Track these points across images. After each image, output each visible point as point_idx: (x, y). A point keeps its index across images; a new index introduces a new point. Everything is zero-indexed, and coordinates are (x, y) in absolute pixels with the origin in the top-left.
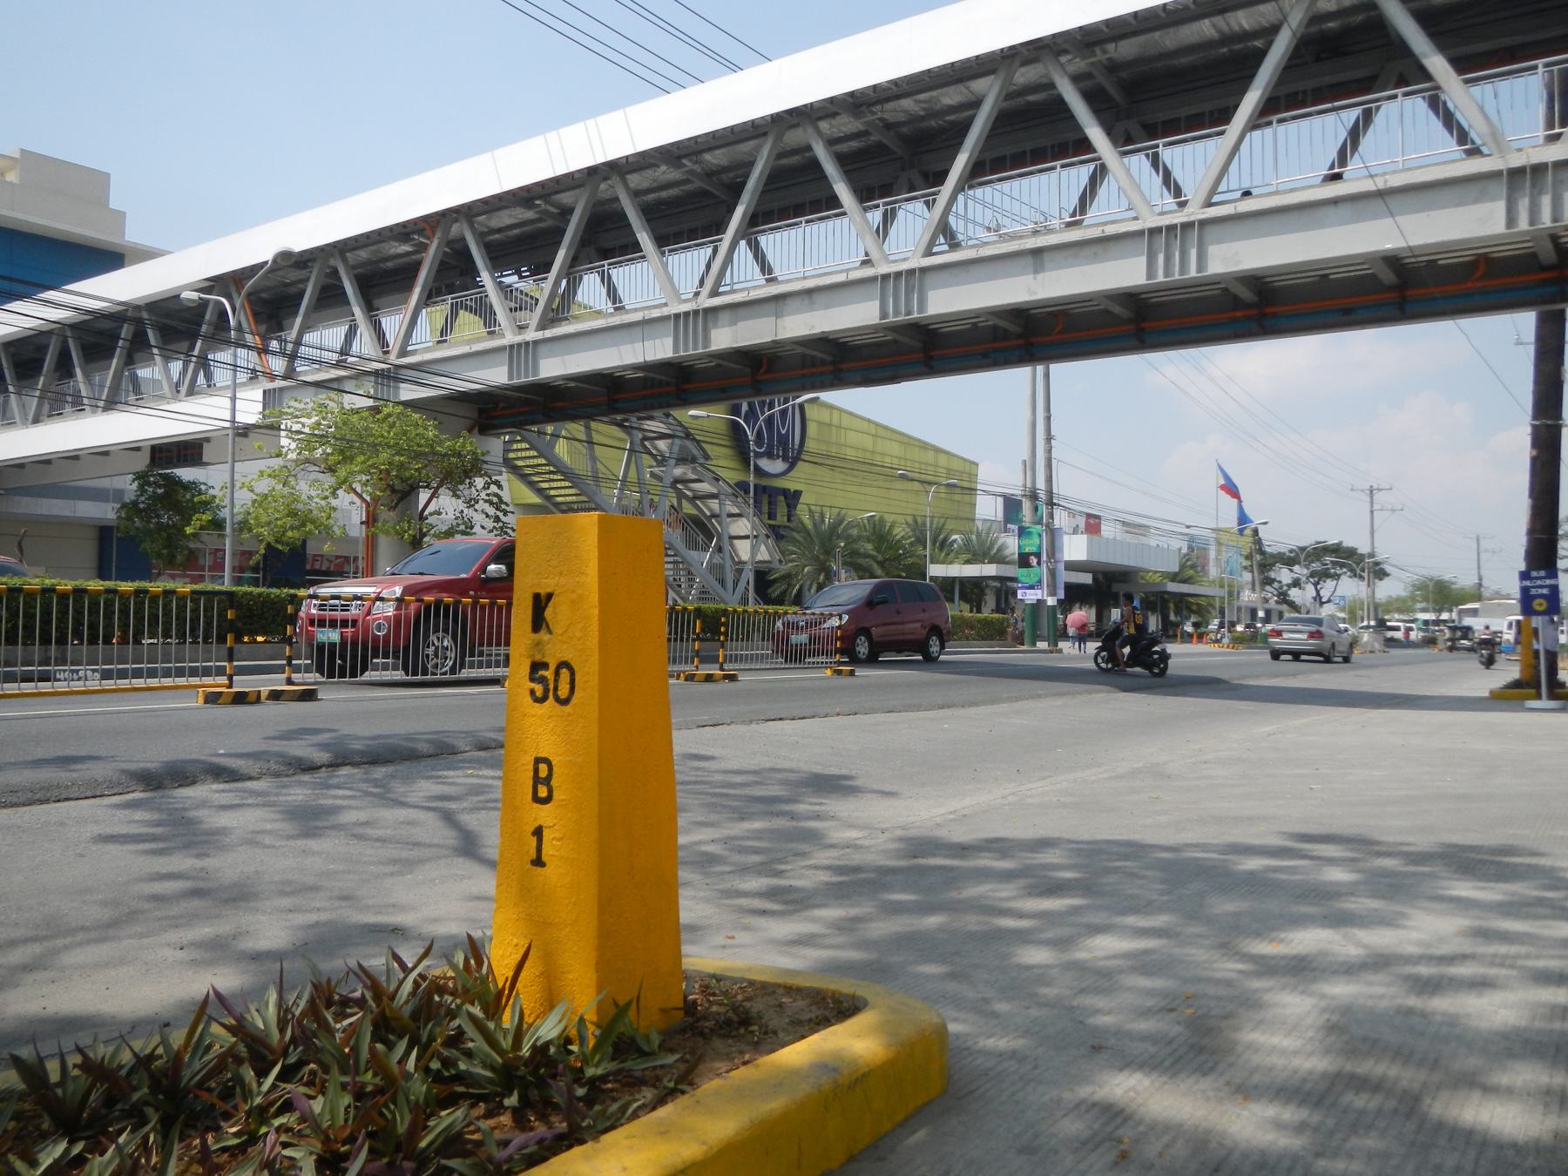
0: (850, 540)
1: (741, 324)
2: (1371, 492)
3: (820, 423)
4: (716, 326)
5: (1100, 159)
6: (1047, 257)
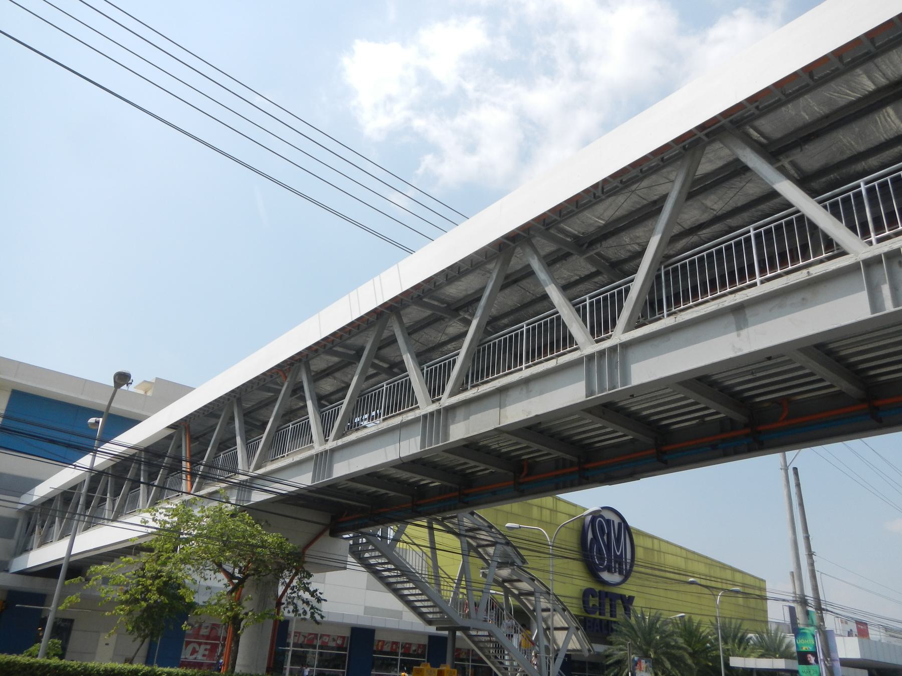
0: (666, 635)
1: (472, 418)
3: (646, 549)
4: (453, 423)
5: (798, 211)
6: (748, 312)
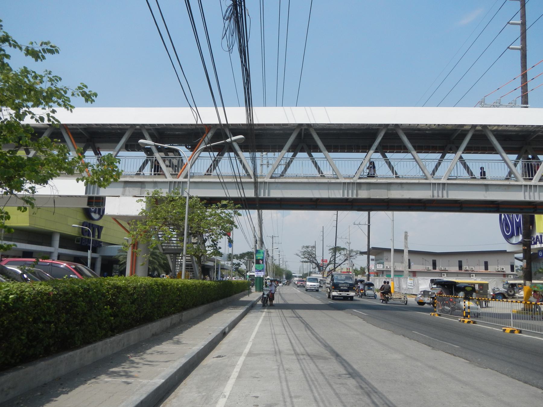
2: (273, 237)
6: (489, 187)
